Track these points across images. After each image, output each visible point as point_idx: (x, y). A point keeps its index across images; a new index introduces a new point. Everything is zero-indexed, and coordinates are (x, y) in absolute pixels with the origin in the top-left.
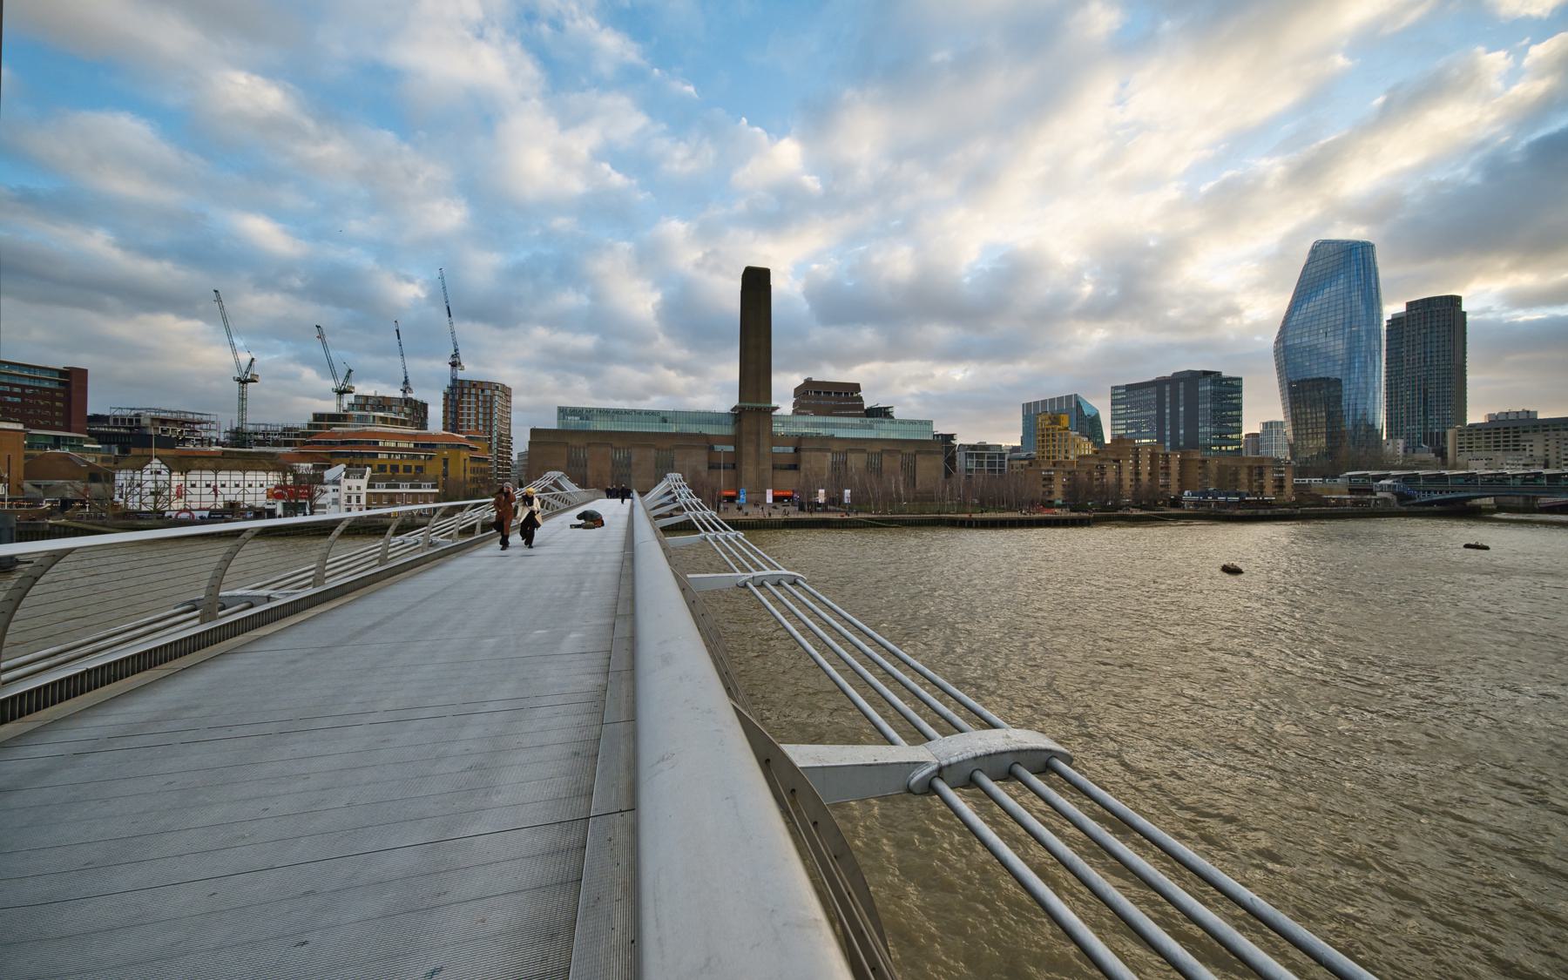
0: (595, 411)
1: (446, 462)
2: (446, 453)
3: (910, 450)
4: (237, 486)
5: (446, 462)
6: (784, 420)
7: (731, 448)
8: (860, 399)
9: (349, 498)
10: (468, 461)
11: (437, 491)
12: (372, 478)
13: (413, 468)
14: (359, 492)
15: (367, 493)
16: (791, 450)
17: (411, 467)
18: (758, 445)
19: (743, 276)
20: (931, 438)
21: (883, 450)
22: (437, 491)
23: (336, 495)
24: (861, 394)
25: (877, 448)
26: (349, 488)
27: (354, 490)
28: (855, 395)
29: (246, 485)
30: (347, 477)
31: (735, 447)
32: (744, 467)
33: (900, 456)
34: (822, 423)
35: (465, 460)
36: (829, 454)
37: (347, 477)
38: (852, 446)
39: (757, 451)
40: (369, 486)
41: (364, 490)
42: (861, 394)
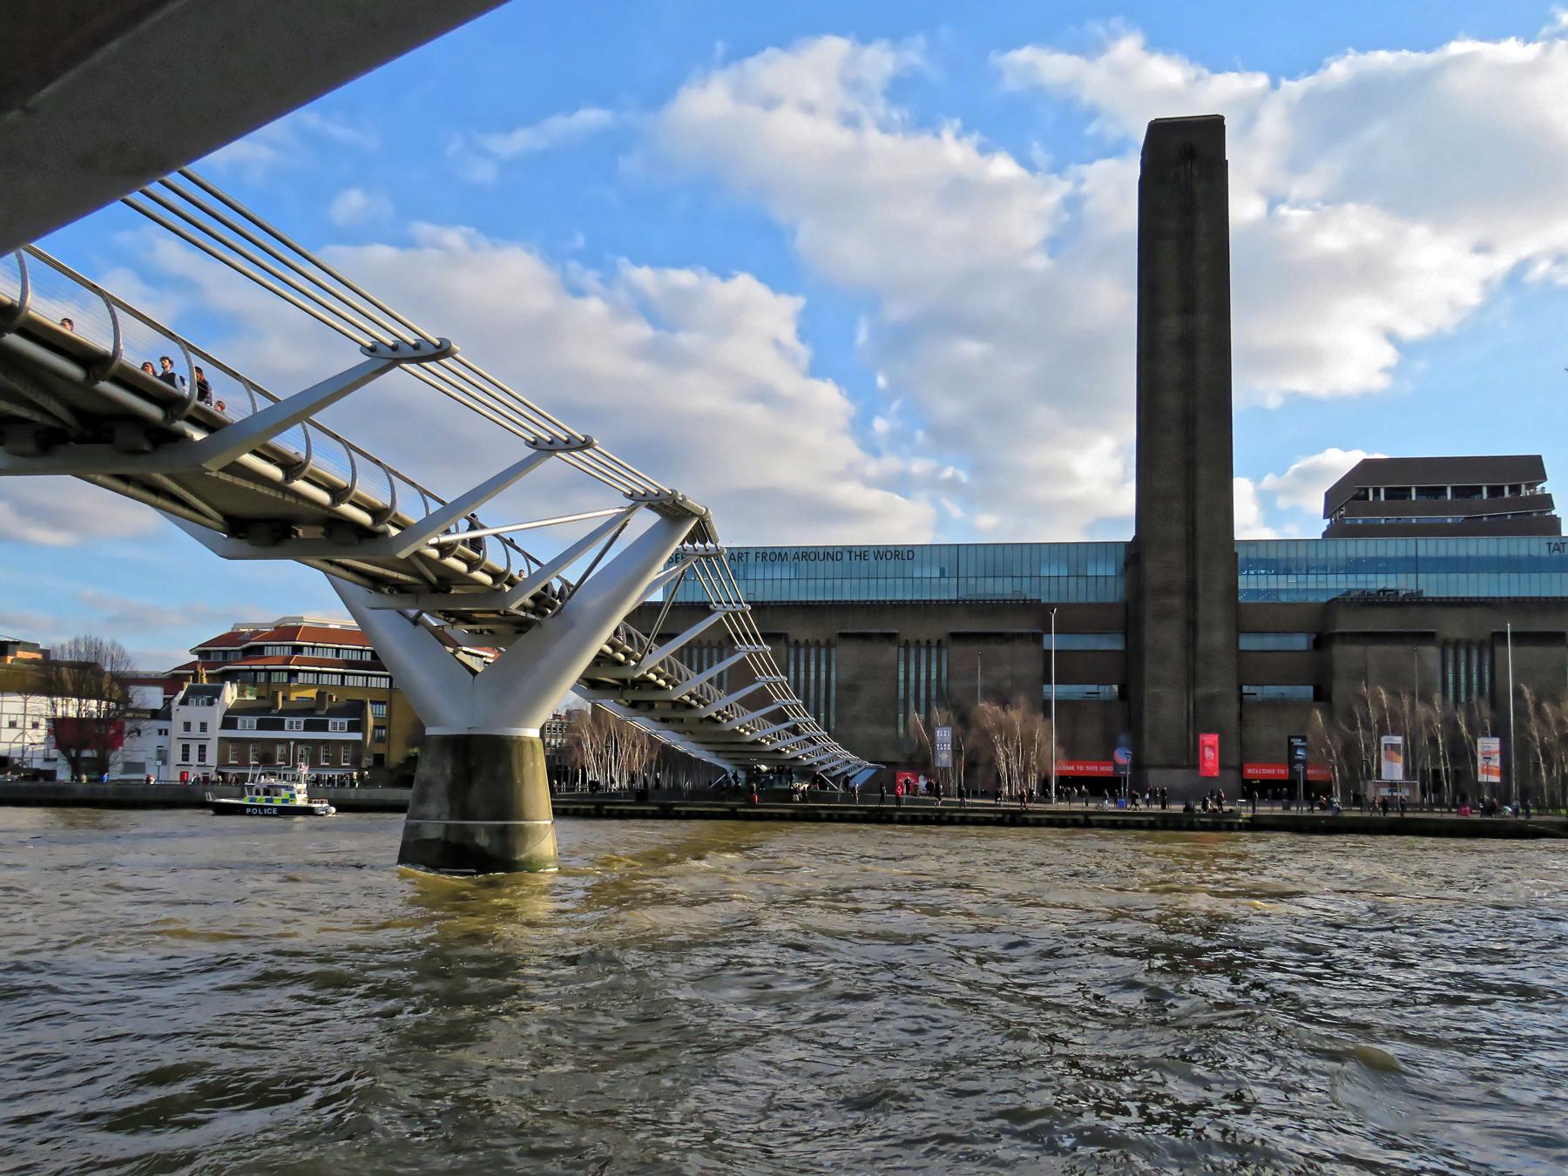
0: (752, 557)
4: (13, 725)
6: (1278, 557)
8: (1547, 501)
9: (186, 748)
14: (203, 735)
15: (221, 739)
16: (1301, 642)
18: (1192, 625)
22: (357, 736)
23: (161, 740)
24: (1547, 487)
26: (187, 726)
27: (196, 728)
28: (1524, 492)
29: (29, 725)
31: (1126, 634)
32: (1150, 691)
34: (1406, 559)
36: (1431, 653)
39: (1190, 643)
41: (216, 732)
42: (1547, 487)
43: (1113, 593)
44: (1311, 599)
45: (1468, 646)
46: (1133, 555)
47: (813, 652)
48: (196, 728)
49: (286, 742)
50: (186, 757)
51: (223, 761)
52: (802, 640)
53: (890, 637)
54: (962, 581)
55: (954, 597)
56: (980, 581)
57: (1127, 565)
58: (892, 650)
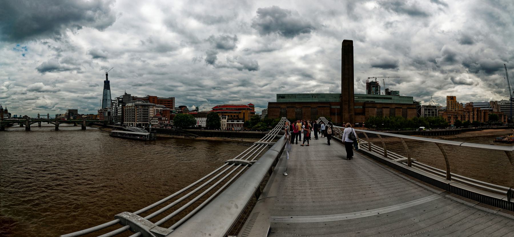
1: (244, 113)
2: (244, 111)
3: (405, 107)
5: (244, 113)
7: (339, 107)
10: (250, 113)
11: (243, 123)
12: (228, 119)
16: (361, 107)
17: (235, 116)
20: (412, 103)
21: (395, 107)
22: (243, 123)
25: (394, 107)
27: (224, 122)
30: (222, 119)
31: (340, 106)
33: (402, 109)
35: (249, 113)
36: (376, 109)
37: (222, 119)
38: (385, 106)
39: (349, 107)
40: (227, 121)
41: (226, 123)
43: (338, 100)
44: (362, 102)
45: (380, 108)
46: (341, 96)
47: (299, 109)
49: (234, 124)
50: (223, 126)
51: (227, 126)
52: (297, 107)
55: (317, 101)
57: (340, 97)
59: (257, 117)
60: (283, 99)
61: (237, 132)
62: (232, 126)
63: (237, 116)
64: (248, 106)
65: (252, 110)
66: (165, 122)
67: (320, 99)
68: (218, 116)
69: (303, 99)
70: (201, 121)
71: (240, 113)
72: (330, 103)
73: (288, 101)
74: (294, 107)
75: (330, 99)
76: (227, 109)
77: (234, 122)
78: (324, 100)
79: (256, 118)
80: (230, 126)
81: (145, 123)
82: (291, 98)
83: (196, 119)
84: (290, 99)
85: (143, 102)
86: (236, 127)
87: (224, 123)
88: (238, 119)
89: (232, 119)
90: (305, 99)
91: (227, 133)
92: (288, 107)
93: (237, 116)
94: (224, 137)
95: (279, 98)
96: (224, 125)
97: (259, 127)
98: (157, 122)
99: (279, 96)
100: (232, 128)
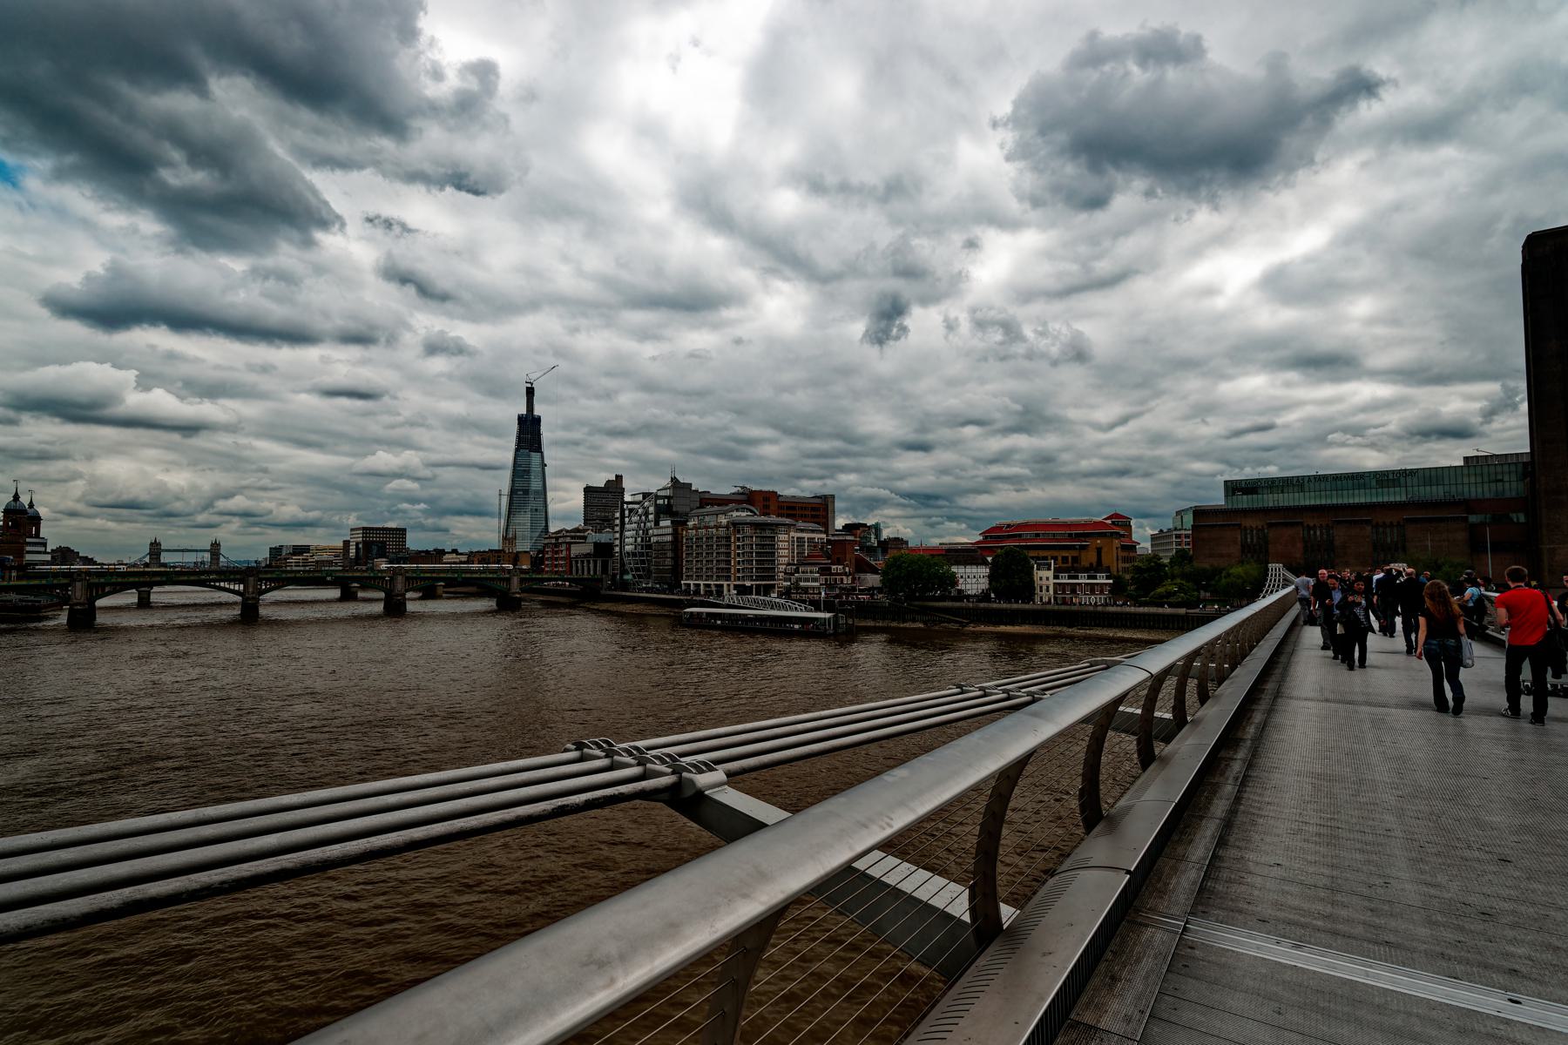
1: (1099, 550)
2: (1099, 542)
5: (1099, 550)
11: (1111, 581)
13: (1070, 558)
17: (1067, 557)
19: (1523, 247)
22: (1111, 581)
27: (1044, 579)
30: (1038, 569)
35: (1117, 548)
37: (1038, 569)
40: (1056, 577)
41: (1052, 581)
43: (1513, 487)
48: (1044, 579)
50: (1041, 591)
51: (1055, 592)
53: (1367, 522)
54: (1410, 489)
55: (1404, 498)
56: (1422, 488)
58: (1369, 528)
59: (1155, 562)
60: (1250, 497)
61: (1100, 609)
62: (1074, 591)
63: (1075, 559)
64: (1109, 522)
65: (1123, 536)
66: (842, 579)
67: (1416, 488)
68: (1026, 560)
69: (1334, 492)
70: (975, 577)
71: (1083, 548)
72: (1469, 505)
73: (1271, 505)
74: (1297, 524)
75: (1466, 489)
76: (1038, 535)
77: (1077, 578)
78: (1437, 492)
79: (1152, 564)
80: (1064, 592)
81: (764, 585)
82: (1282, 492)
83: (954, 569)
84: (1281, 495)
85: (751, 511)
86: (1085, 594)
87: (1044, 582)
88: (1092, 570)
89: (1073, 570)
90: (1345, 492)
91: (1066, 611)
92: (1271, 525)
93: (1072, 557)
94: (1054, 625)
95: (1234, 494)
96: (1044, 588)
97: (1169, 594)
98: (815, 580)
99: (1232, 488)
100: (1072, 598)
